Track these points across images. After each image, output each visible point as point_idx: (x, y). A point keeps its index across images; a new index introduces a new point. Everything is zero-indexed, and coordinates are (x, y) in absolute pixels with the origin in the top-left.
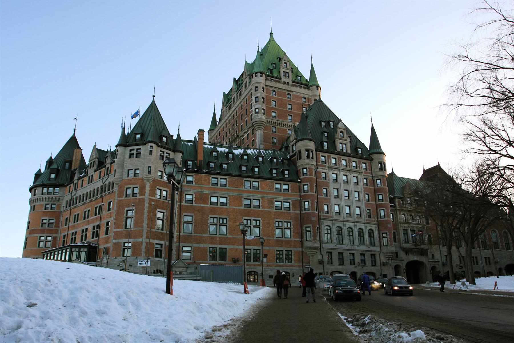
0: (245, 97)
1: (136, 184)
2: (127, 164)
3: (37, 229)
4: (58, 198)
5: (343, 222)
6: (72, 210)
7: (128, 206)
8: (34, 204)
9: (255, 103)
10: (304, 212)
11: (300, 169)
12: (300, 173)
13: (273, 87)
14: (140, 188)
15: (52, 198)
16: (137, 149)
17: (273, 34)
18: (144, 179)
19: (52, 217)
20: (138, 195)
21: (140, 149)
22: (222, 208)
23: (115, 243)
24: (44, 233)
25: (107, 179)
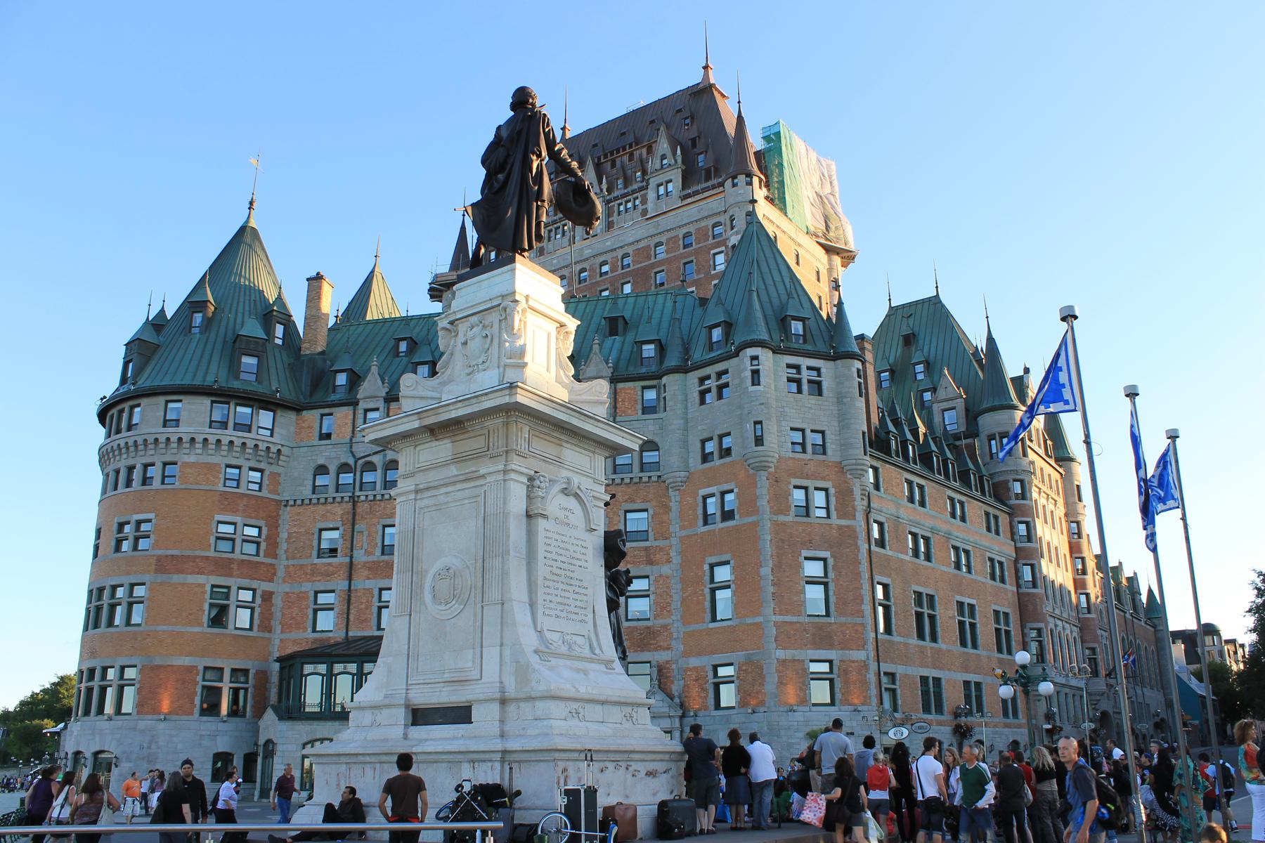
0: (680, 227)
1: (823, 479)
2: (786, 409)
4: (274, 449)
5: (1054, 617)
6: (360, 509)
7: (809, 544)
8: (168, 458)
10: (1023, 590)
11: (1008, 481)
12: (1009, 489)
13: (773, 223)
14: (836, 492)
16: (809, 368)
19: (257, 518)
20: (834, 514)
21: (818, 370)
22: (926, 568)
23: (784, 661)
24: (230, 575)
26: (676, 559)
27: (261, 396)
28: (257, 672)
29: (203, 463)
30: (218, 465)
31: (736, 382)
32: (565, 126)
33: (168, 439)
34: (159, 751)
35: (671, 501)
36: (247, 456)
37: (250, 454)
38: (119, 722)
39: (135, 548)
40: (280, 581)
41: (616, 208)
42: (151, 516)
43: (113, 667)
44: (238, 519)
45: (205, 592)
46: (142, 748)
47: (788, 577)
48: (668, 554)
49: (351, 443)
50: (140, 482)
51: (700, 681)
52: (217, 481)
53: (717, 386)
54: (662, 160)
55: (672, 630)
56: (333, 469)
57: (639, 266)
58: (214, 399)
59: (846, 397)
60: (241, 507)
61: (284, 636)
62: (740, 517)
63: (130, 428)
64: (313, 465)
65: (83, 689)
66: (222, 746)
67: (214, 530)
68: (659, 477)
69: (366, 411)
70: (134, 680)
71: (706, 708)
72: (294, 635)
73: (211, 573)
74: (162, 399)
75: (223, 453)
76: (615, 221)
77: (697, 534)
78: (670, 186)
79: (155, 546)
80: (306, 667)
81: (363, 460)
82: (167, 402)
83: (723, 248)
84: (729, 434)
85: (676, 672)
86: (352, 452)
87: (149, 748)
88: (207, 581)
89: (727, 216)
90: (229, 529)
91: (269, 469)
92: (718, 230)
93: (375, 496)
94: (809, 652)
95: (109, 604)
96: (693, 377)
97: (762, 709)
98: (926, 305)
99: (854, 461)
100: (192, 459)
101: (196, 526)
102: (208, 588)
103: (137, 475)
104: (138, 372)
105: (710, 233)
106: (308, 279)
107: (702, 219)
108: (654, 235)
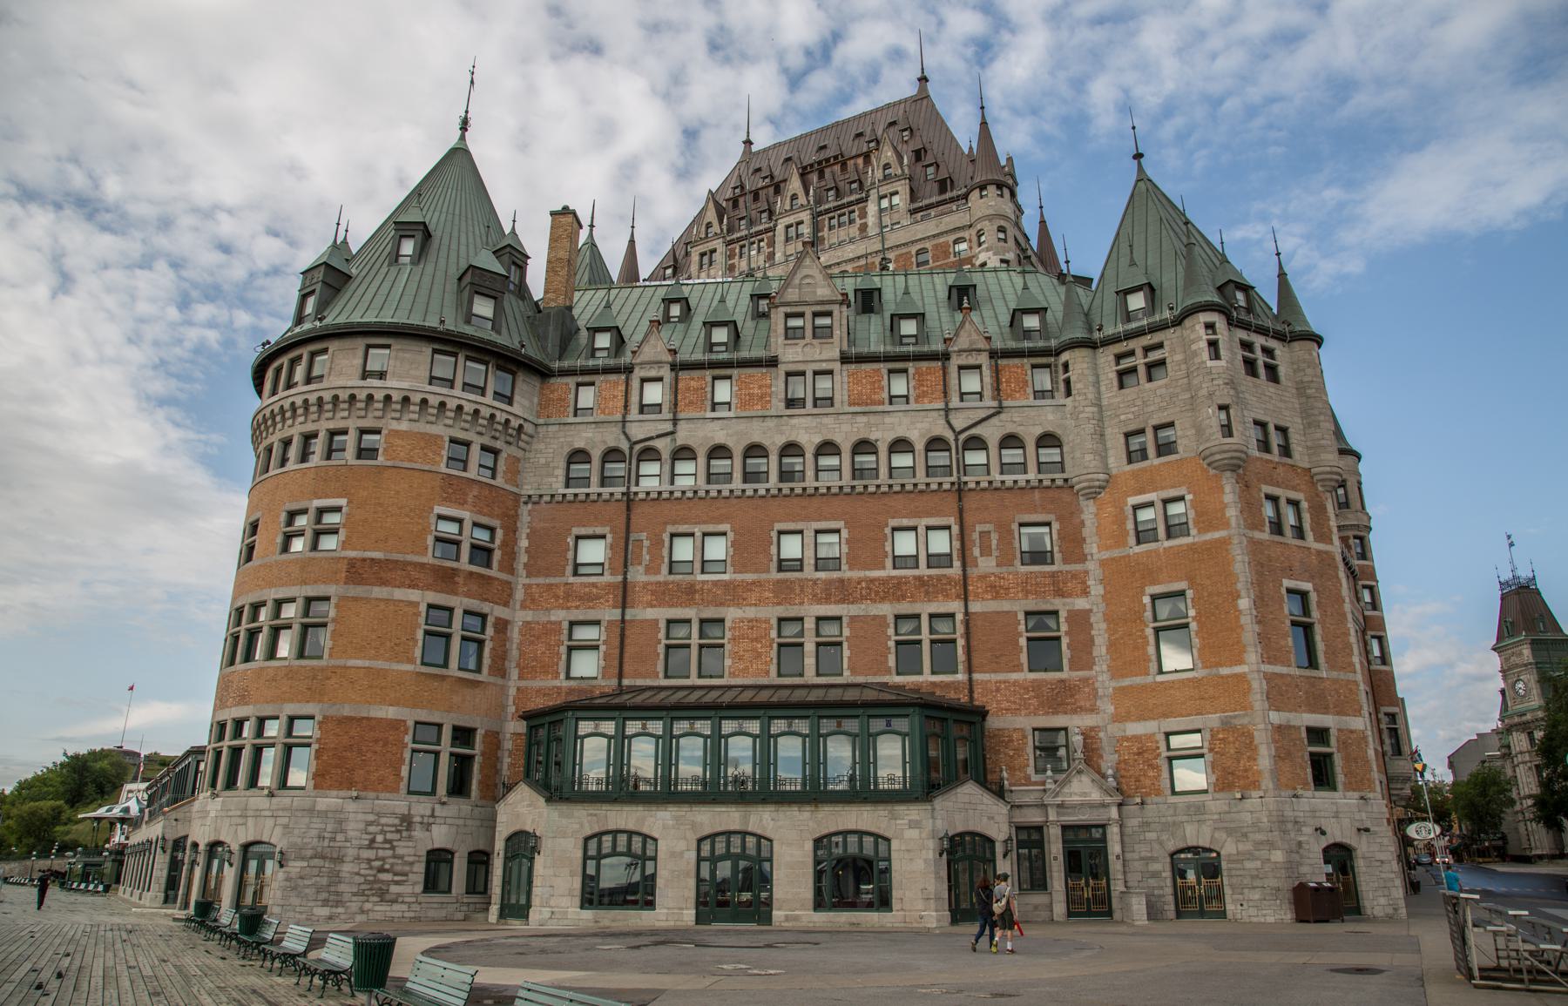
0: (913, 242)
1: (1294, 488)
2: (1247, 396)
3: (410, 563)
4: (515, 423)
7: (1290, 572)
14: (1310, 507)
15: (493, 416)
17: (927, 81)
18: (1316, 478)
19: (490, 516)
20: (1309, 535)
24: (454, 593)
26: (1096, 590)
27: (500, 348)
28: (487, 734)
29: (418, 433)
30: (441, 437)
31: (1179, 357)
33: (370, 397)
34: (348, 844)
36: (479, 429)
37: (484, 426)
38: (283, 800)
39: (314, 546)
40: (518, 606)
42: (342, 502)
43: (277, 718)
44: (466, 515)
45: (418, 614)
46: (321, 838)
47: (1271, 613)
48: (1084, 583)
49: (624, 422)
50: (325, 455)
51: (1146, 755)
52: (438, 459)
53: (1146, 364)
54: (885, 169)
55: (1097, 685)
56: (596, 455)
58: (437, 347)
59: (1309, 388)
60: (470, 499)
61: (523, 683)
62: (1199, 532)
63: (309, 380)
64: (567, 450)
65: (225, 751)
66: (440, 836)
67: (433, 528)
68: (1066, 480)
69: (644, 380)
70: (310, 737)
71: (1158, 793)
73: (427, 587)
74: (361, 343)
76: (826, 236)
77: (1129, 556)
78: (896, 200)
79: (345, 545)
80: (582, 724)
81: (642, 445)
82: (369, 347)
85: (1105, 743)
86: (625, 433)
87: (333, 839)
88: (422, 597)
89: (973, 232)
90: (450, 529)
91: (507, 451)
92: (963, 246)
94: (1306, 716)
95: (271, 627)
96: (1106, 357)
97: (1255, 794)
99: (1328, 469)
100: (404, 426)
101: (408, 520)
102: (423, 608)
103: (318, 446)
104: (319, 314)
105: (951, 250)
106: (553, 214)
107: (942, 233)
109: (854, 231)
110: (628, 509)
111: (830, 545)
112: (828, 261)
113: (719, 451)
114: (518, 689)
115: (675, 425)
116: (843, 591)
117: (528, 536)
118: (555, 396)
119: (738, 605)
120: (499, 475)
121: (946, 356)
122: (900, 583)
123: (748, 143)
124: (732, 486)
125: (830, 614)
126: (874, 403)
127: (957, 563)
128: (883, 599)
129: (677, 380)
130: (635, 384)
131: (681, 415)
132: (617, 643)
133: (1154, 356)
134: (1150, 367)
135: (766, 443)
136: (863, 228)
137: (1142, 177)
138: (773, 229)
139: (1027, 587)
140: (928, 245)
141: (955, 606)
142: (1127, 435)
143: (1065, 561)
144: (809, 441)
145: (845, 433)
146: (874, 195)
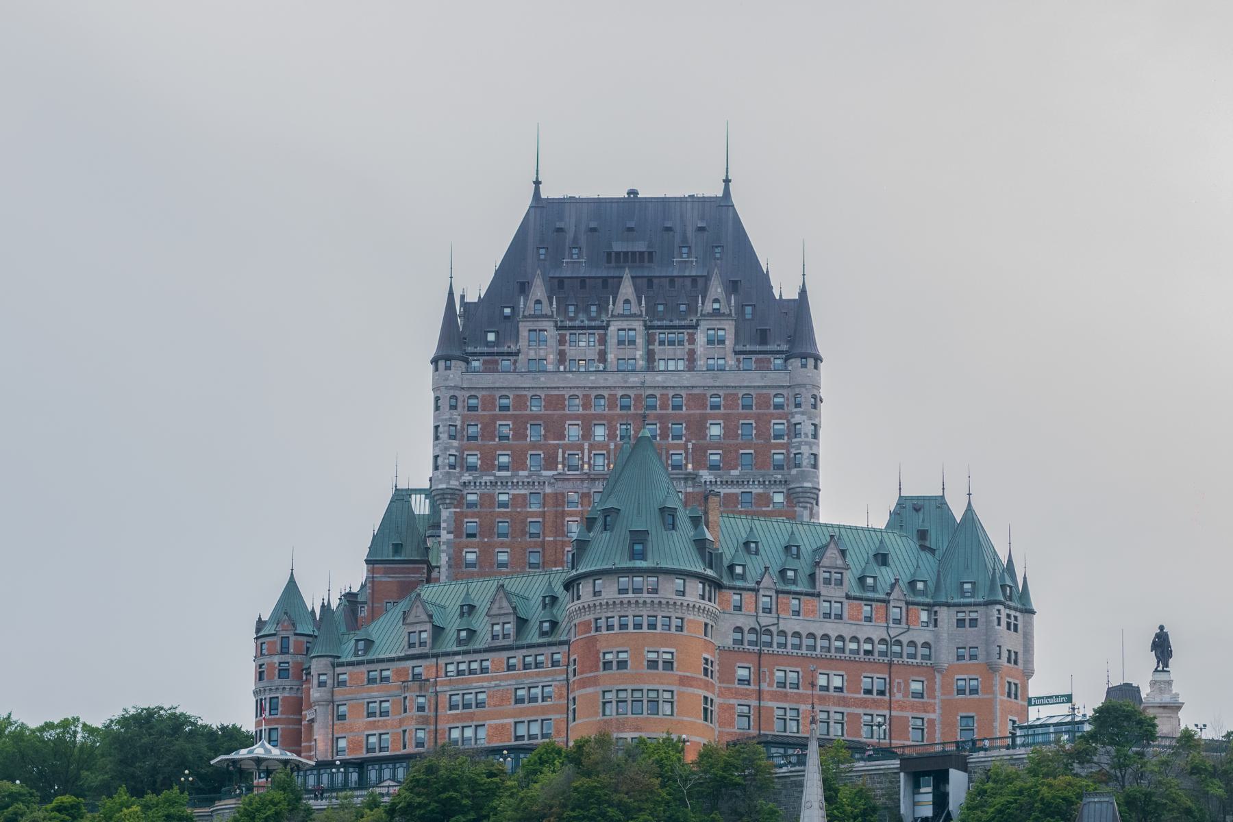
0: (740, 387)
1: (1017, 679)
7: (1011, 713)
8: (679, 615)
9: (810, 439)
20: (1019, 698)
25: (904, 633)
26: (938, 711)
32: (537, 178)
33: (682, 604)
35: (935, 678)
41: (657, 337)
49: (757, 616)
57: (692, 412)
68: (931, 664)
72: (727, 730)
75: (670, 610)
83: (785, 421)
84: (977, 648)
86: (758, 622)
91: (714, 627)
93: (773, 651)
98: (932, 502)
100: (691, 617)
107: (766, 386)
108: (712, 387)
109: (681, 351)
110: (760, 657)
111: (837, 682)
112: (664, 382)
113: (797, 634)
114: (719, 732)
115: (778, 620)
116: (845, 702)
117: (718, 665)
118: (725, 598)
119: (805, 704)
120: (713, 638)
121: (889, 602)
122: (866, 701)
123: (537, 183)
124: (802, 652)
125: (839, 711)
126: (859, 620)
127: (888, 695)
128: (860, 707)
129: (777, 598)
130: (761, 596)
131: (781, 616)
132: (758, 715)
133: (973, 615)
134: (970, 620)
135: (816, 633)
136: (692, 353)
137: (969, 508)
138: (606, 328)
139: (913, 707)
140: (753, 392)
141: (886, 712)
142: (958, 648)
143: (928, 698)
144: (833, 635)
145: (847, 632)
146: (704, 325)
